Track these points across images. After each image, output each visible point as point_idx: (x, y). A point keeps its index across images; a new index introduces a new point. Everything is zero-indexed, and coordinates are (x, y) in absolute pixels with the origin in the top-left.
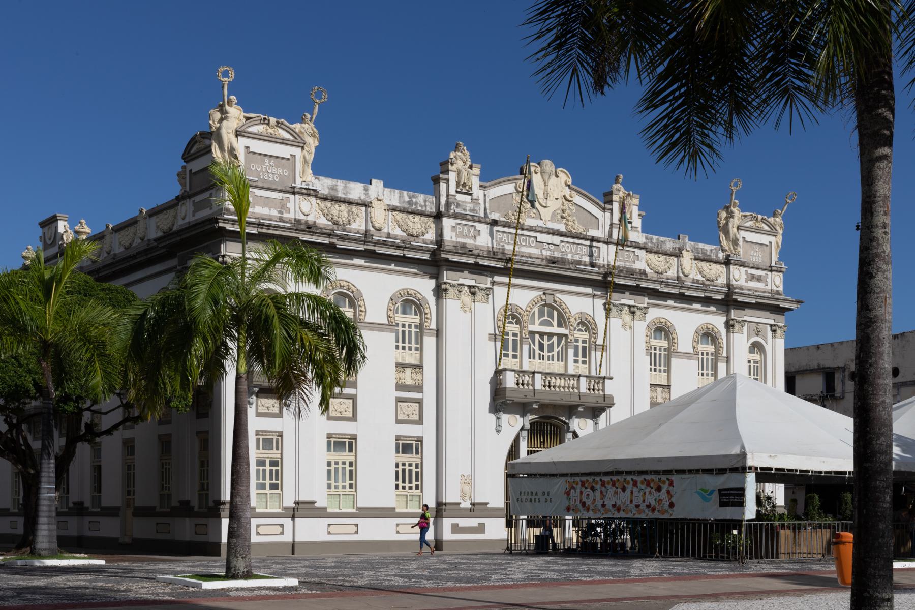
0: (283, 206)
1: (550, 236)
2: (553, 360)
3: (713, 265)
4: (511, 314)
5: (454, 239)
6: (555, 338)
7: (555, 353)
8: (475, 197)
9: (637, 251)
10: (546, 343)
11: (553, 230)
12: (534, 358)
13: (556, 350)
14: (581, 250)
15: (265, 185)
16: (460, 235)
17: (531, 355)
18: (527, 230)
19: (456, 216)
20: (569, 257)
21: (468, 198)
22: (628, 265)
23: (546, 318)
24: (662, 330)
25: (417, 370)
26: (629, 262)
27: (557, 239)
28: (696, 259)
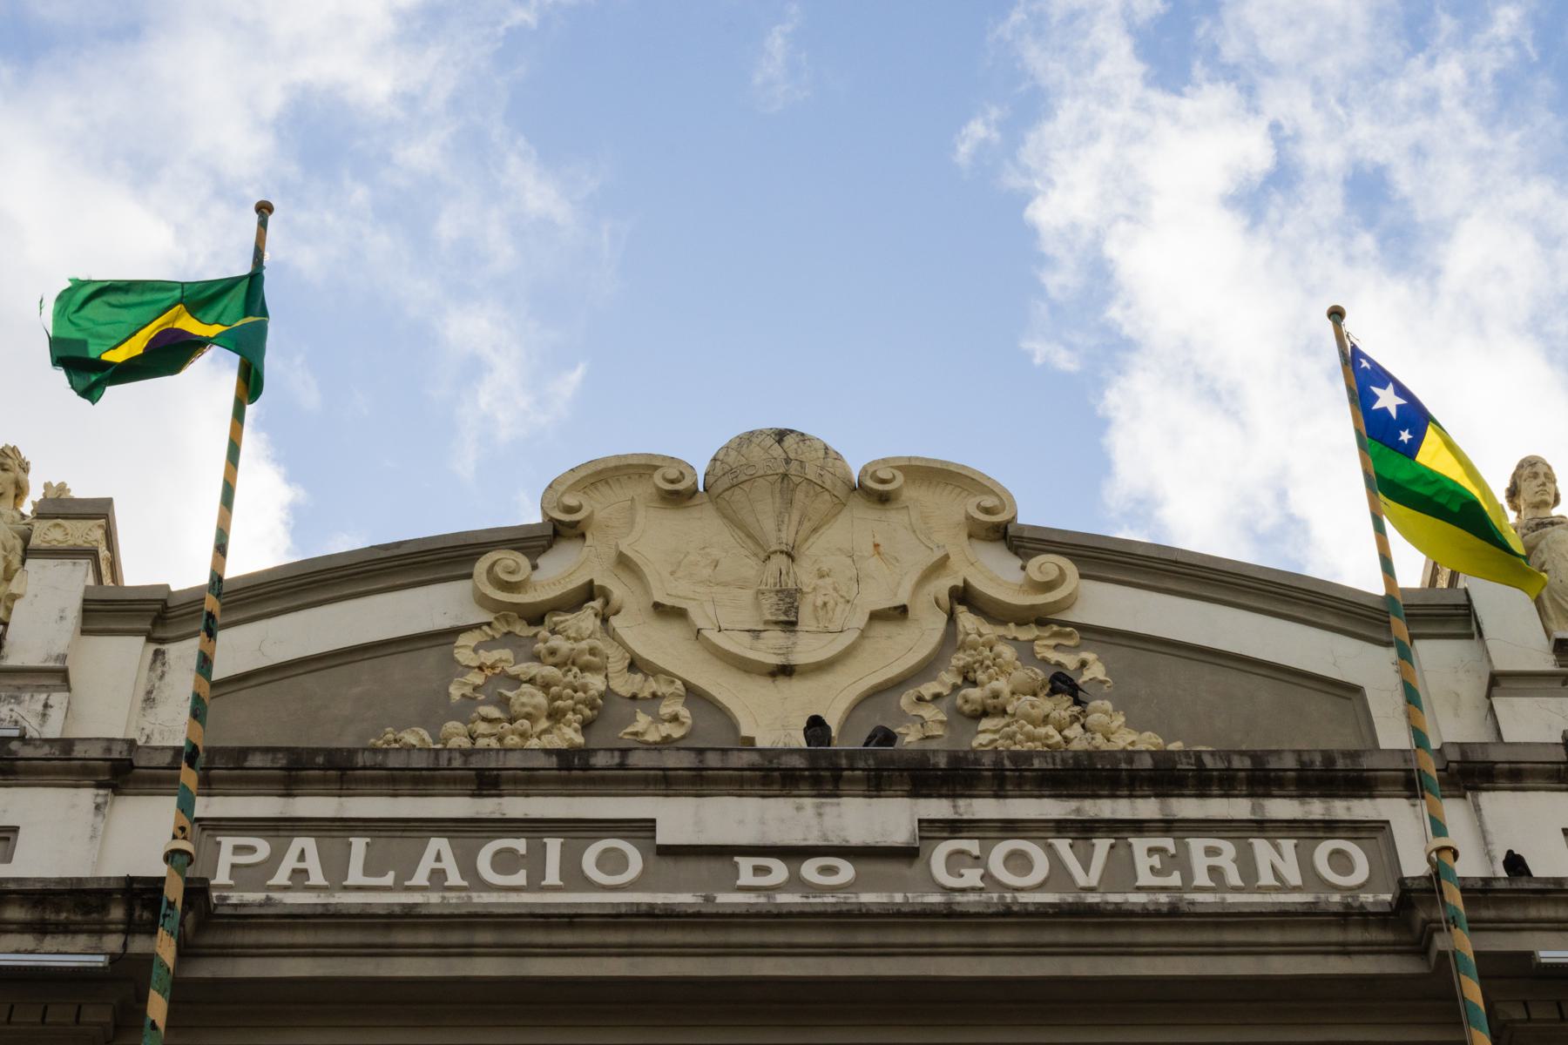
14: (1180, 862)
18: (529, 781)
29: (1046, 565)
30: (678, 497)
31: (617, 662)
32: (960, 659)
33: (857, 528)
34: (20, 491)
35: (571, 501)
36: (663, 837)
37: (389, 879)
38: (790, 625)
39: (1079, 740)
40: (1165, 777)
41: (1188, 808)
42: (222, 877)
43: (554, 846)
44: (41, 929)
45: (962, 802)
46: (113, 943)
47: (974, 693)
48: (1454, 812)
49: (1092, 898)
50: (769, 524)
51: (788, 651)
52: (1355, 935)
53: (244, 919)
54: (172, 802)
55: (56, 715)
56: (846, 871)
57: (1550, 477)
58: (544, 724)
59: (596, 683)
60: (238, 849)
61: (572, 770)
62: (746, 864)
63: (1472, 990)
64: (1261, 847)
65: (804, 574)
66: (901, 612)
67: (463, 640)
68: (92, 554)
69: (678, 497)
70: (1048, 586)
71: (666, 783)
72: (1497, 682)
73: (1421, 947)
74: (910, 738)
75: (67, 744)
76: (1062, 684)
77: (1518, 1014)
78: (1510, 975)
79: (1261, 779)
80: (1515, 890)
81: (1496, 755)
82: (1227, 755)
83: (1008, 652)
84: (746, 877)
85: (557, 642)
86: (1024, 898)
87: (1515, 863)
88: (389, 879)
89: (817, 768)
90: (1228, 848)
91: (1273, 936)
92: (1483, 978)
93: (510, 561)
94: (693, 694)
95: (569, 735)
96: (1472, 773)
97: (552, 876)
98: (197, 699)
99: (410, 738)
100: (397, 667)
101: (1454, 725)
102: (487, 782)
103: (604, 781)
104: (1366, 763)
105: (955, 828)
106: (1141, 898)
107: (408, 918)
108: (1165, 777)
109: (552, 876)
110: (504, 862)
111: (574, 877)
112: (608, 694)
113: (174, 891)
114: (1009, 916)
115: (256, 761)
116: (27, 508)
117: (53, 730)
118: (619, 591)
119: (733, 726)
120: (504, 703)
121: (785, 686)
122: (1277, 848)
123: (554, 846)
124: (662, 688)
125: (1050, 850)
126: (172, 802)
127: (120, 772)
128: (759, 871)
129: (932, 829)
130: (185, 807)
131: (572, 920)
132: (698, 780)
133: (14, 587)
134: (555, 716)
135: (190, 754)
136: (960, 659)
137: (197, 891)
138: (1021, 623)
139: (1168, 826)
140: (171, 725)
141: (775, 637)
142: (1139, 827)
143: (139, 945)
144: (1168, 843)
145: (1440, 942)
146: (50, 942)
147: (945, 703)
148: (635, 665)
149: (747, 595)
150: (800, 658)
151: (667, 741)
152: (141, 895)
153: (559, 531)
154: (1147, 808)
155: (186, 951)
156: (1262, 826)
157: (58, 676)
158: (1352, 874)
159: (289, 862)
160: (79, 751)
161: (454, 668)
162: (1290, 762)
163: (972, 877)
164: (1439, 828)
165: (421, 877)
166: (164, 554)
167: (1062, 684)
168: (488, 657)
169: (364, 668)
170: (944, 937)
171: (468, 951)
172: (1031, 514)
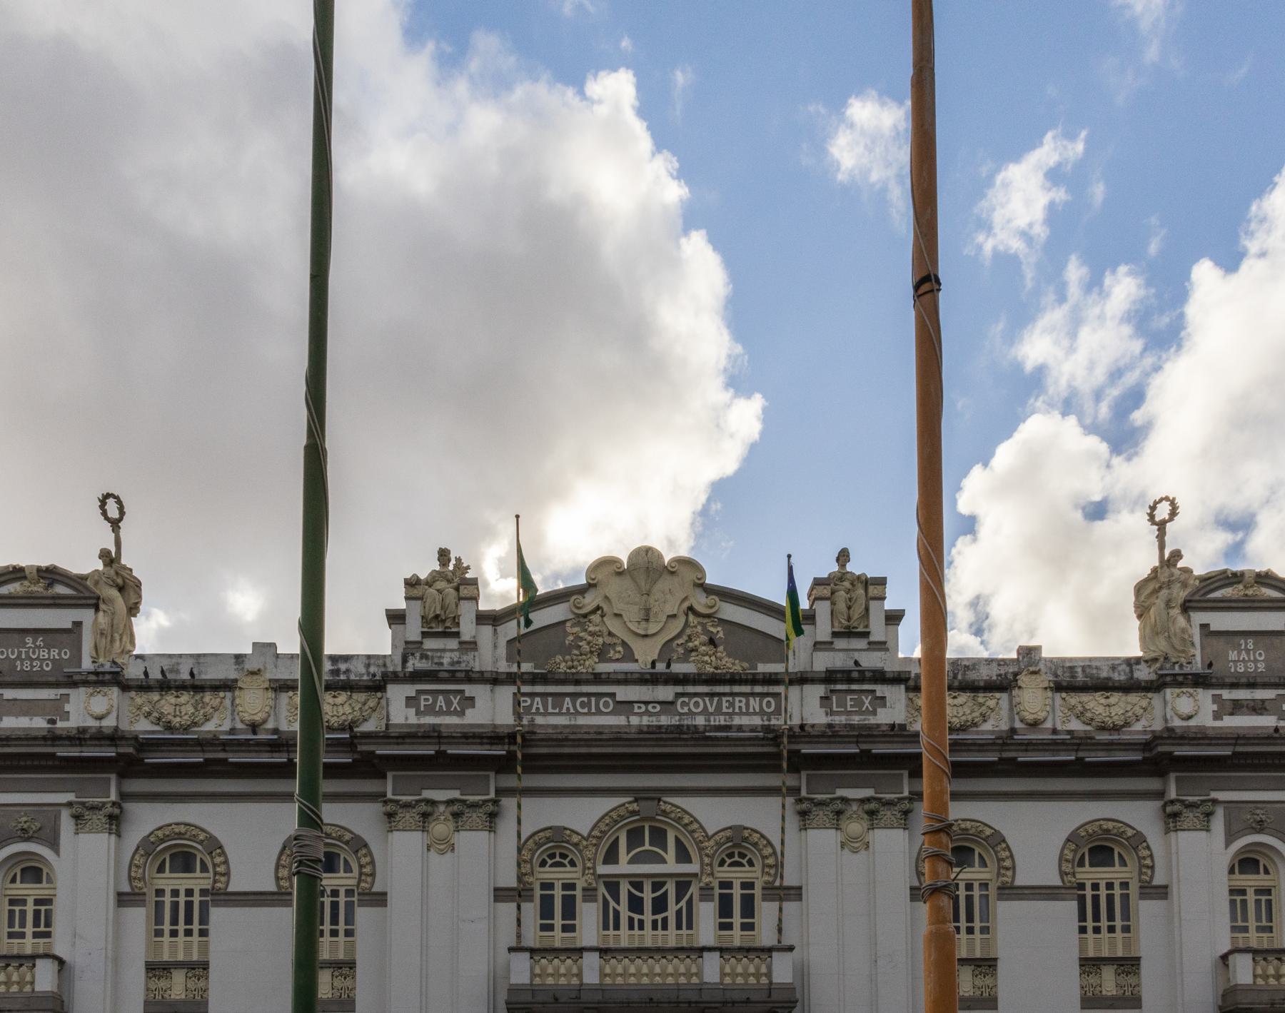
0: (56, 709)
1: (644, 689)
2: (665, 927)
3: (1115, 697)
4: (555, 846)
5: (413, 720)
6: (671, 887)
8: (466, 637)
9: (880, 690)
10: (648, 896)
11: (685, 675)
12: (617, 927)
13: (672, 907)
14: (732, 705)
15: (17, 679)
16: (430, 710)
17: (609, 921)
18: (587, 682)
19: (416, 677)
20: (700, 721)
21: (453, 644)
22: (856, 719)
23: (647, 847)
24: (959, 847)
25: (345, 971)
26: (860, 713)
27: (666, 693)
28: (1058, 687)
33: (665, 583)
36: (618, 699)
38: (647, 620)
41: (737, 689)
43: (593, 699)
46: (506, 747)
47: (690, 644)
51: (646, 629)
56: (658, 708)
59: (601, 640)
62: (636, 705)
64: (751, 699)
66: (674, 616)
70: (711, 607)
72: (818, 646)
76: (712, 642)
90: (744, 700)
102: (577, 682)
105: (683, 695)
119: (633, 654)
129: (678, 695)
139: (732, 694)
141: (643, 624)
142: (725, 694)
148: (610, 634)
150: (650, 632)
153: (590, 586)
154: (726, 689)
156: (753, 694)
161: (566, 634)
167: (712, 642)
172: (709, 580)
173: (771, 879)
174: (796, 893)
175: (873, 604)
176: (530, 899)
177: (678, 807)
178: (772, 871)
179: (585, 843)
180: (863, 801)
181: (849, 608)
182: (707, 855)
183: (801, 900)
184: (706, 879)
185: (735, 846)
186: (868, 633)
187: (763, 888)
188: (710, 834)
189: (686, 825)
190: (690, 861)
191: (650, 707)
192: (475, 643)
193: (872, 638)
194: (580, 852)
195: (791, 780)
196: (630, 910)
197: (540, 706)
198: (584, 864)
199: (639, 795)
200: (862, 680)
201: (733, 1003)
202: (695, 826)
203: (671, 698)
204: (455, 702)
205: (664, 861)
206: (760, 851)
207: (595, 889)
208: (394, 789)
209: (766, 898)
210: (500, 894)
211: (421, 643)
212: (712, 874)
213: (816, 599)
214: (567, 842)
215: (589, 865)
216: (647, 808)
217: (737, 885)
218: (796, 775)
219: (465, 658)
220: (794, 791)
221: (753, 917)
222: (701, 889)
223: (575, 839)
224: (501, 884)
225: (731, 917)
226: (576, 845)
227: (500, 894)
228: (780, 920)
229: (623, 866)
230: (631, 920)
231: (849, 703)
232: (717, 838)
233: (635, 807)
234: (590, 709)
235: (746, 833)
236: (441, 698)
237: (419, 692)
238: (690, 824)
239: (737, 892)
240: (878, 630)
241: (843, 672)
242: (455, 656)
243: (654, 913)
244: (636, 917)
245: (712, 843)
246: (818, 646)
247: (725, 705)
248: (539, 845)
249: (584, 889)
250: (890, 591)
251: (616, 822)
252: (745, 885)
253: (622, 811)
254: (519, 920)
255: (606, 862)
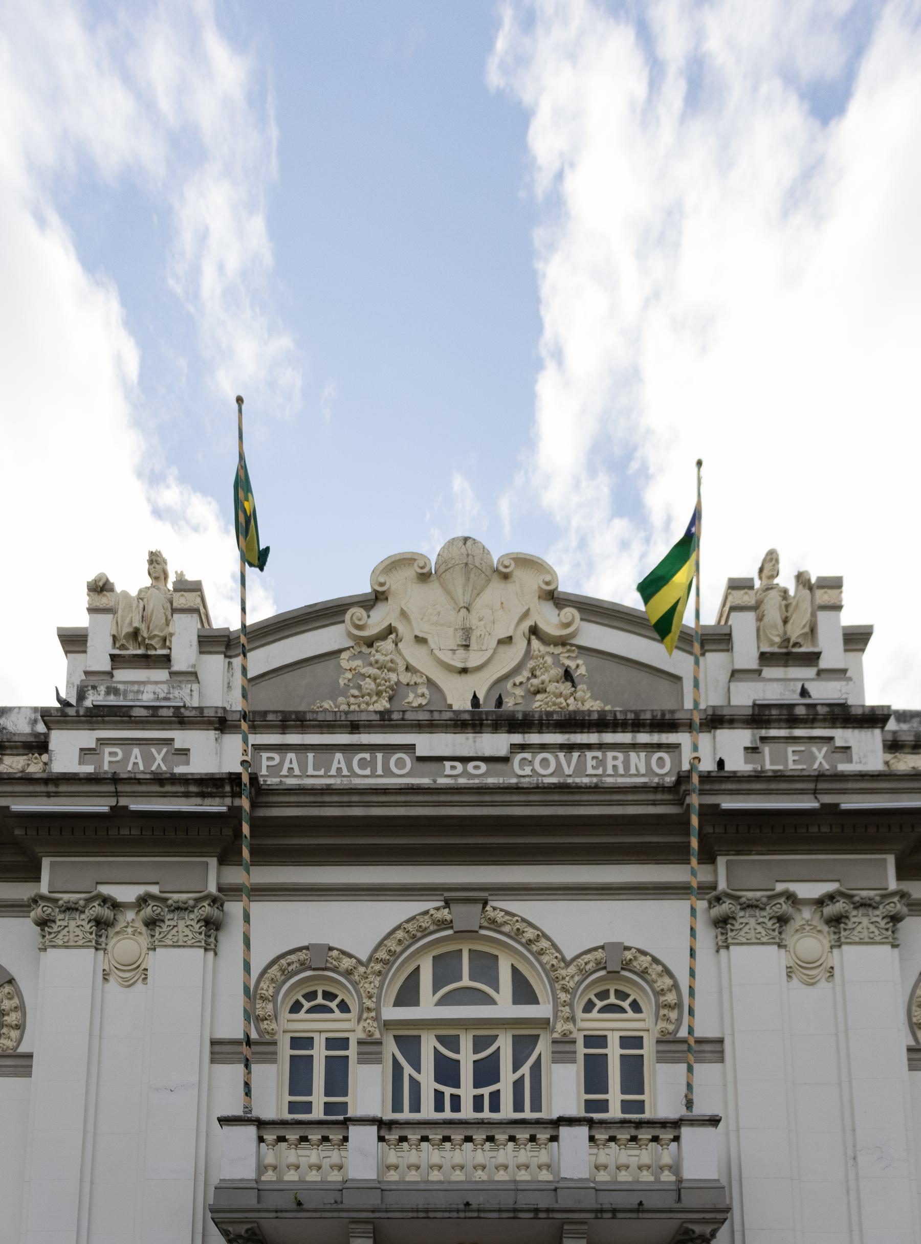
4: (314, 976)
6: (505, 1044)
7: (505, 1085)
10: (467, 1058)
13: (507, 1077)
14: (602, 763)
23: (466, 982)
27: (496, 743)
29: (570, 612)
30: (424, 577)
31: (401, 667)
32: (531, 664)
34: (166, 577)
35: (382, 580)
36: (419, 753)
37: (322, 772)
39: (573, 706)
40: (603, 724)
41: (609, 738)
42: (264, 772)
44: (202, 795)
45: (526, 735)
48: (704, 739)
49: (570, 780)
50: (460, 591)
52: (659, 797)
53: (272, 791)
54: (240, 736)
55: (196, 694)
56: (483, 767)
57: (777, 561)
58: (375, 698)
60: (269, 759)
61: (385, 721)
62: (448, 764)
63: (695, 821)
64: (633, 755)
65: (473, 621)
67: (345, 655)
68: (197, 611)
69: (424, 577)
71: (419, 727)
72: (735, 674)
73: (681, 802)
74: (509, 704)
75: (201, 709)
77: (710, 830)
78: (710, 813)
79: (637, 725)
80: (719, 778)
81: (726, 712)
82: (625, 712)
83: (549, 660)
84: (448, 771)
85: (378, 656)
86: (547, 780)
87: (721, 764)
88: (322, 772)
89: (473, 721)
90: (620, 756)
91: (630, 797)
92: (701, 815)
93: (357, 612)
94: (430, 682)
95: (383, 704)
96: (716, 721)
97: (379, 771)
98: (243, 688)
99: (326, 705)
100: (318, 669)
101: (712, 698)
102: (354, 727)
103: (396, 726)
104: (678, 716)
105: (523, 747)
106: (586, 780)
107: (327, 790)
108: (603, 724)
109: (379, 771)
110: (363, 764)
111: (388, 772)
112: (398, 683)
113: (245, 779)
114: (539, 789)
115: (270, 717)
116: (170, 586)
117: (195, 704)
118: (401, 628)
120: (359, 687)
121: (466, 678)
122: (638, 756)
123: (379, 756)
124: (419, 680)
125: (557, 757)
126: (240, 736)
127: (222, 723)
128: (453, 768)
130: (245, 741)
131: (385, 791)
132: (430, 726)
133: (171, 629)
134: (379, 694)
135: (244, 716)
136: (531, 664)
137: (254, 778)
138: (556, 645)
139: (601, 746)
140: (236, 703)
142: (589, 747)
143: (237, 802)
144: (599, 754)
145: (688, 800)
146: (208, 801)
147: (524, 686)
149: (452, 630)
151: (420, 706)
152: (234, 779)
154: (592, 738)
155: (254, 805)
156: (634, 746)
157: (193, 675)
158: (662, 769)
159: (287, 765)
160: (206, 713)
162: (648, 716)
163: (528, 770)
164: (695, 748)
165: (333, 772)
166: (225, 616)
168: (354, 664)
169: (307, 669)
170: (515, 798)
171: (350, 804)
173: (671, 1028)
174: (713, 1049)
175: (822, 616)
176: (270, 1058)
177: (513, 915)
178: (673, 1015)
179: (362, 969)
180: (820, 902)
181: (785, 621)
182: (564, 989)
183: (722, 1060)
184: (561, 1027)
185: (613, 974)
186: (817, 655)
187: (658, 1042)
188: (569, 957)
189: (530, 942)
190: (534, 1000)
191: (471, 765)
192: (195, 674)
193: (824, 663)
194: (355, 984)
195: (704, 874)
196: (437, 1079)
197: (295, 765)
198: (361, 1004)
199: (451, 896)
200: (811, 720)
201: (614, 1211)
202: (544, 944)
203: (503, 752)
204: (159, 758)
205: (492, 1002)
206: (650, 983)
207: (379, 1043)
208: (51, 884)
209: (662, 1057)
210: (220, 1050)
211: (110, 674)
212: (572, 1019)
213: (733, 609)
214: (335, 970)
215: (369, 1003)
216: (466, 916)
217: (614, 1041)
218: (707, 868)
219: (176, 693)
220: (707, 889)
221: (642, 1092)
222: (555, 1042)
223: (346, 963)
224: (224, 1033)
225: (606, 1092)
226: (348, 973)
227: (220, 1050)
228: (689, 1086)
229: (428, 1007)
230: (439, 1095)
231: (791, 758)
232: (580, 961)
233: (445, 914)
234: (374, 770)
235: (628, 955)
236: (136, 751)
237: (102, 742)
238: (534, 941)
239: (614, 1052)
240: (832, 654)
241: (781, 706)
242: (162, 690)
243: (476, 1085)
244: (448, 1091)
245: (572, 969)
246: (735, 674)
247: (590, 763)
248: (287, 974)
249: (360, 1043)
250: (847, 596)
251: (415, 939)
252: (627, 1042)
253: (425, 922)
254: (247, 1085)
255: (397, 1004)
